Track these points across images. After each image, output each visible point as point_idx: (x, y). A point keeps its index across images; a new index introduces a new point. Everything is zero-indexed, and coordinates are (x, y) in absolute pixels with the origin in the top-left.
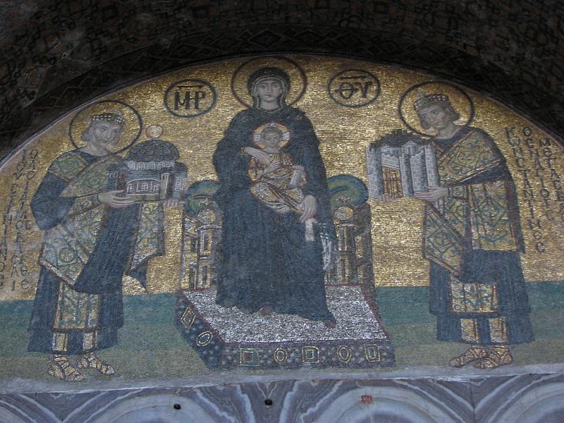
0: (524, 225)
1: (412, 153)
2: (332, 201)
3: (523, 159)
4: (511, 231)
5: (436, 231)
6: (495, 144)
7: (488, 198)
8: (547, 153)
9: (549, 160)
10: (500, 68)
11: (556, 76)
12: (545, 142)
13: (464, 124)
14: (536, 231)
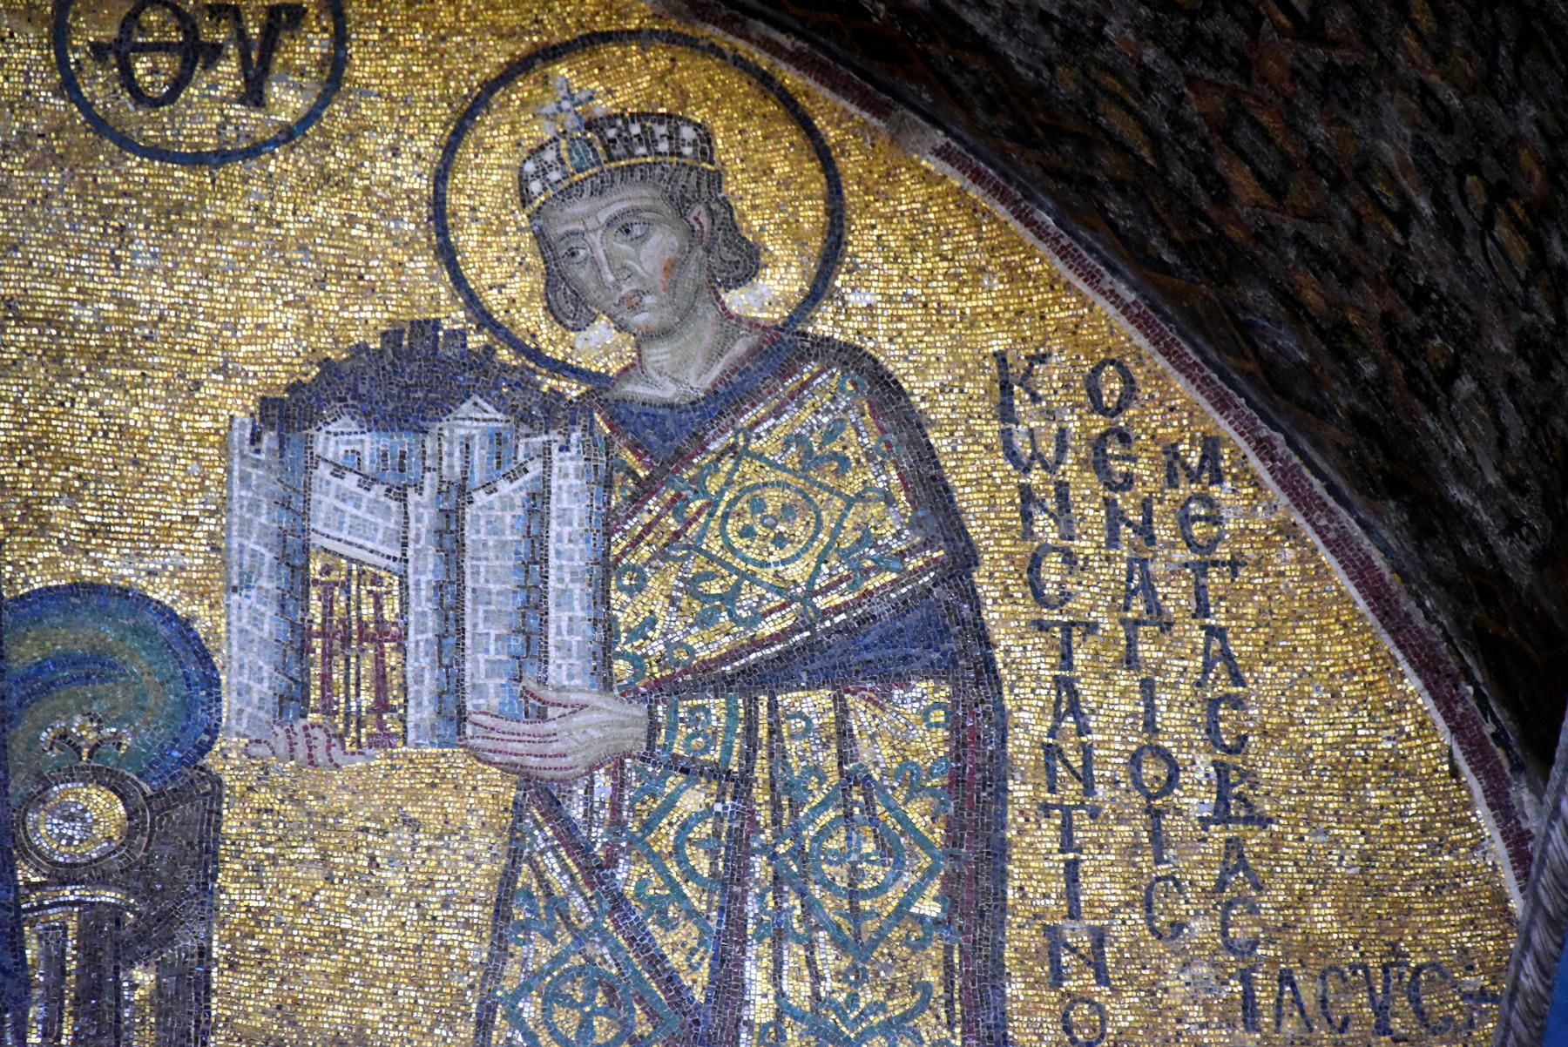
0: (1023, 954)
1: (477, 477)
2: (17, 748)
3: (1069, 557)
4: (948, 985)
5: (556, 960)
6: (928, 455)
7: (854, 778)
8: (1197, 530)
9: (1201, 569)
10: (986, 37)
11: (1250, 163)
12: (1194, 460)
13: (778, 314)
14: (1075, 999)
